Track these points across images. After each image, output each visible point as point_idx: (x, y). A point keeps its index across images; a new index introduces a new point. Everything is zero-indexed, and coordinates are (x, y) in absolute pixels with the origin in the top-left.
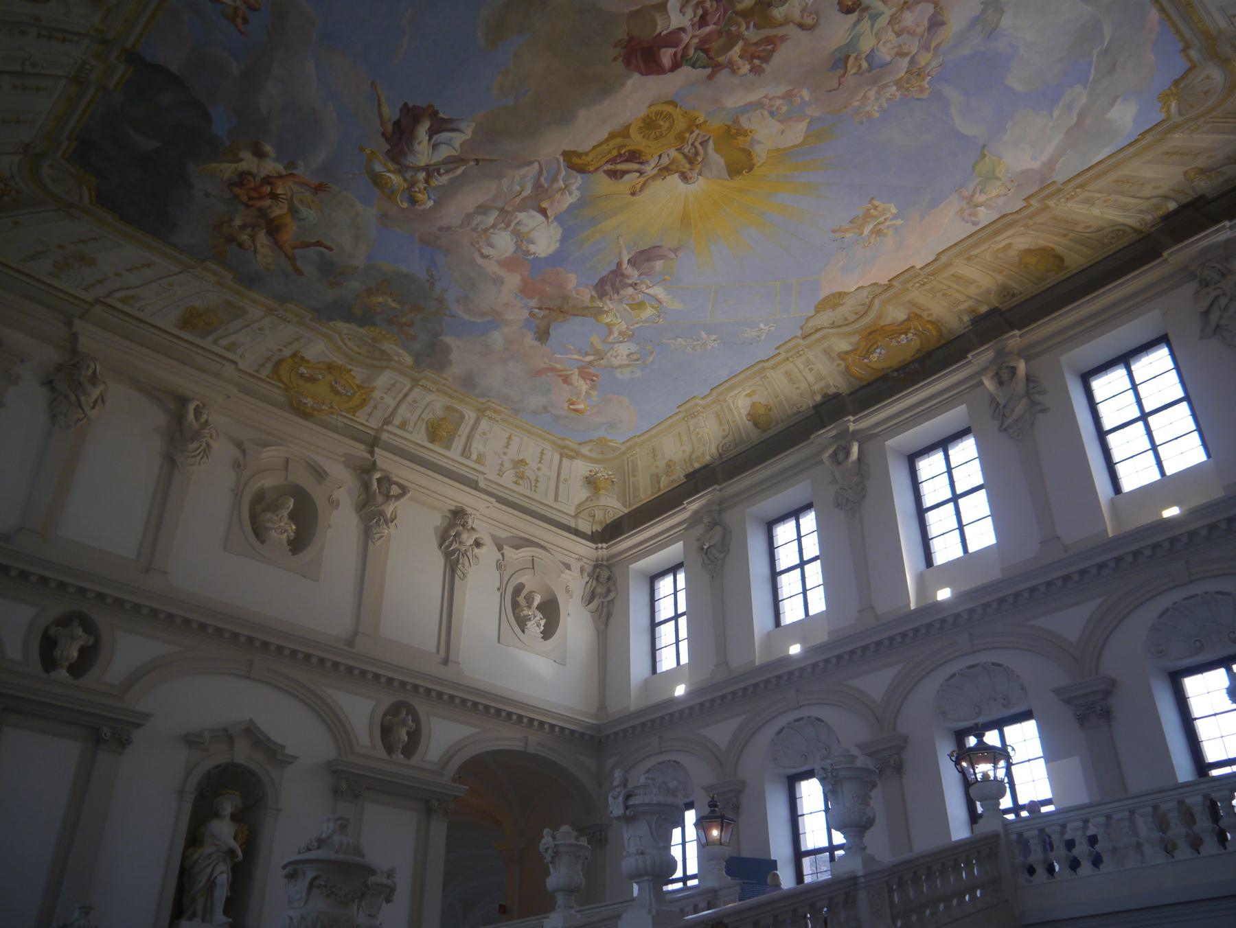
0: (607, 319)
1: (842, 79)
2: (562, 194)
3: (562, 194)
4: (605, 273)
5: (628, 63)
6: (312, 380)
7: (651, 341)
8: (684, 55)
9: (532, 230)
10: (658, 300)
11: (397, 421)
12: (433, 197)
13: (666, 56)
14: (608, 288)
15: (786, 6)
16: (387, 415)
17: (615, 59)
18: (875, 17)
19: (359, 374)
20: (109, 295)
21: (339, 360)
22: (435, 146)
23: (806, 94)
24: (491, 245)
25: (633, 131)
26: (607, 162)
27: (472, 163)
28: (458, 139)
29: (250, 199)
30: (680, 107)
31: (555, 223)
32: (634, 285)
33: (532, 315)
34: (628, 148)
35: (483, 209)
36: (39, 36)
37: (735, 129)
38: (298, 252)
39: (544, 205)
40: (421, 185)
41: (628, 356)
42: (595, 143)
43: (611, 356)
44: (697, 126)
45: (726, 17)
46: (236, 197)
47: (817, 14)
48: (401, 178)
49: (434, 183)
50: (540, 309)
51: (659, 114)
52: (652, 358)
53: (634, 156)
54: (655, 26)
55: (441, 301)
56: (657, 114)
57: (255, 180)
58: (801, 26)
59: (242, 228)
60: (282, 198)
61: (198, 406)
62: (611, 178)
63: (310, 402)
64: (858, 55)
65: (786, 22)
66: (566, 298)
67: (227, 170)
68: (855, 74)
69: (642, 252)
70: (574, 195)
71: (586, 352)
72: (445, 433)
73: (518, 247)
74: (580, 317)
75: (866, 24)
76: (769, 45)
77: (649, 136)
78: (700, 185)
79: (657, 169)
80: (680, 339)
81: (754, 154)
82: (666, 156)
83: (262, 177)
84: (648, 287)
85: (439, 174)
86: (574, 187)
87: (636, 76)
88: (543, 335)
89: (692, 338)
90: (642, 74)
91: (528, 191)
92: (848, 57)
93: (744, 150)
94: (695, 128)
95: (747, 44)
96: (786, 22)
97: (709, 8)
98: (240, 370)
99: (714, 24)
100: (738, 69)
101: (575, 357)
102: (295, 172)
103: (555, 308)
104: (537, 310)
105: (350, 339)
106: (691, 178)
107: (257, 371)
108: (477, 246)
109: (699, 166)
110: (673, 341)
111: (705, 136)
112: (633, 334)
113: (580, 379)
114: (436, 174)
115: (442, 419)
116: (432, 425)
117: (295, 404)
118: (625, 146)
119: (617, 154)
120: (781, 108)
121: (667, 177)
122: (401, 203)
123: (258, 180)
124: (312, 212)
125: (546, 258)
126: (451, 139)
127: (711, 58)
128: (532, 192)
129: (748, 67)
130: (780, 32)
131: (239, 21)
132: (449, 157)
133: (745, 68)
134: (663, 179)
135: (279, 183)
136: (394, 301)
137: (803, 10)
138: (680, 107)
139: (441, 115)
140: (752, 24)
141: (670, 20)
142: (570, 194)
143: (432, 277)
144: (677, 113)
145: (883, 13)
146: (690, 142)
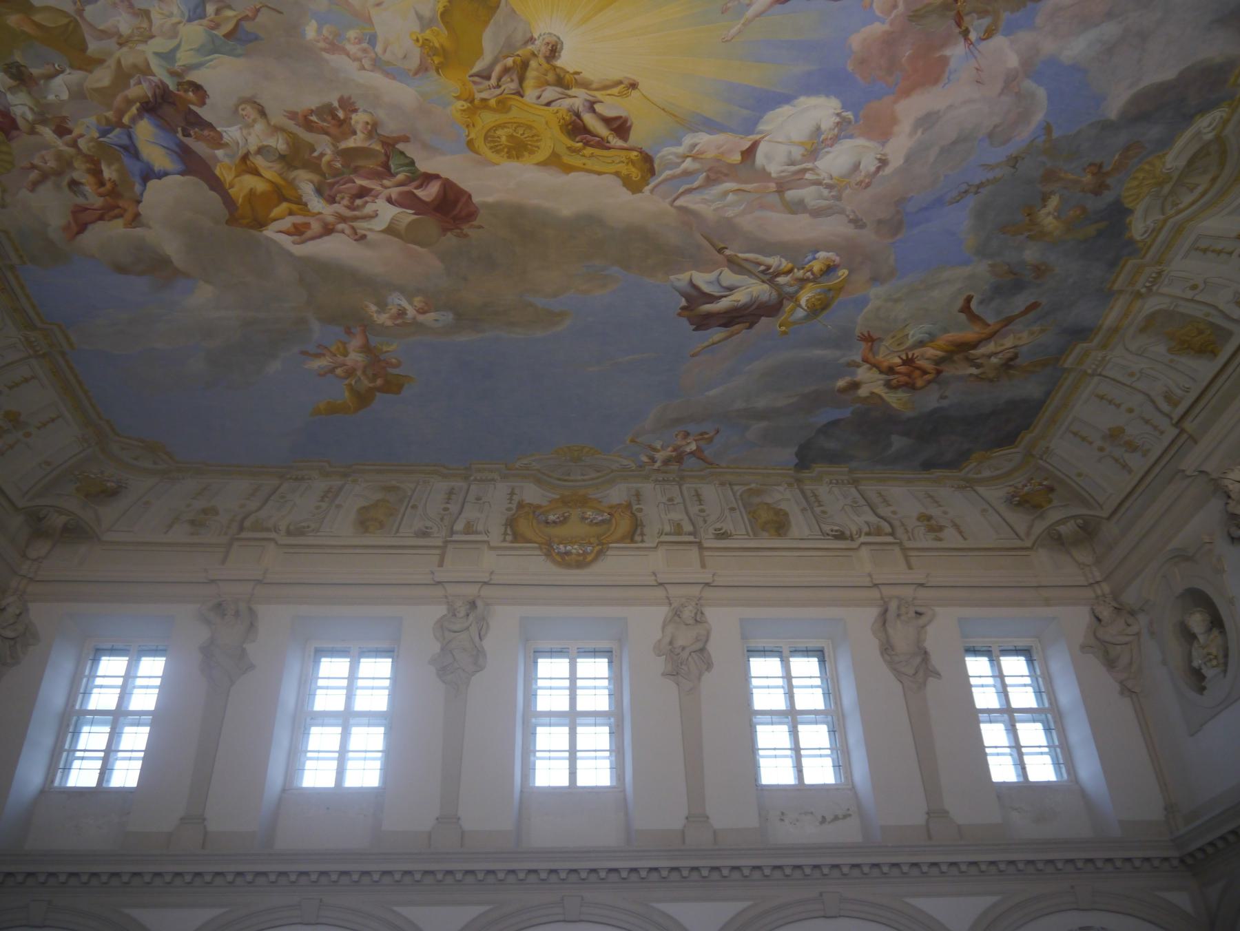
1: (250, 14)
2: (702, 153)
12: (810, 257)
13: (429, 193)
15: (265, 143)
17: (480, 227)
18: (169, 57)
20: (1169, 416)
22: (731, 289)
23: (311, 31)
24: (856, 167)
25: (542, 155)
26: (609, 148)
27: (728, 252)
28: (703, 280)
30: (468, 136)
31: (761, 127)
33: (989, 34)
34: (570, 143)
35: (797, 207)
37: (432, 60)
39: (737, 158)
40: (799, 274)
42: (595, 177)
44: (472, 101)
45: (338, 179)
47: (236, 111)
48: (802, 292)
49: (785, 265)
50: (965, 34)
51: (496, 150)
53: (576, 129)
54: (414, 221)
55: (1014, 161)
56: (498, 152)
58: (263, 113)
59: (978, 366)
62: (630, 127)
64: (213, 28)
65: (278, 129)
67: (895, 400)
68: (229, 7)
70: (696, 140)
73: (836, 139)
75: (183, 58)
76: (312, 121)
77: (533, 136)
78: (545, 26)
79: (570, 92)
82: (542, 97)
86: (681, 150)
87: (476, 199)
90: (470, 196)
91: (729, 185)
92: (228, 36)
93: (446, 23)
94: (476, 102)
95: (336, 140)
96: (278, 129)
97: (347, 198)
99: (354, 182)
100: (367, 123)
103: (953, 13)
104: (973, 36)
106: (548, 44)
108: (867, 180)
109: (518, 53)
111: (474, 83)
114: (771, 271)
118: (569, 148)
120: (356, 38)
121: (571, 71)
122: (840, 277)
123: (891, 377)
124: (911, 333)
126: (710, 283)
129: (354, 116)
130: (291, 125)
131: (706, 436)
132: (735, 273)
133: (359, 119)
135: (886, 364)
136: (1045, 206)
137: (249, 126)
138: (468, 136)
139: (683, 302)
140: (316, 154)
141: (394, 216)
143: (966, 192)
145: (156, 54)
146: (498, 91)
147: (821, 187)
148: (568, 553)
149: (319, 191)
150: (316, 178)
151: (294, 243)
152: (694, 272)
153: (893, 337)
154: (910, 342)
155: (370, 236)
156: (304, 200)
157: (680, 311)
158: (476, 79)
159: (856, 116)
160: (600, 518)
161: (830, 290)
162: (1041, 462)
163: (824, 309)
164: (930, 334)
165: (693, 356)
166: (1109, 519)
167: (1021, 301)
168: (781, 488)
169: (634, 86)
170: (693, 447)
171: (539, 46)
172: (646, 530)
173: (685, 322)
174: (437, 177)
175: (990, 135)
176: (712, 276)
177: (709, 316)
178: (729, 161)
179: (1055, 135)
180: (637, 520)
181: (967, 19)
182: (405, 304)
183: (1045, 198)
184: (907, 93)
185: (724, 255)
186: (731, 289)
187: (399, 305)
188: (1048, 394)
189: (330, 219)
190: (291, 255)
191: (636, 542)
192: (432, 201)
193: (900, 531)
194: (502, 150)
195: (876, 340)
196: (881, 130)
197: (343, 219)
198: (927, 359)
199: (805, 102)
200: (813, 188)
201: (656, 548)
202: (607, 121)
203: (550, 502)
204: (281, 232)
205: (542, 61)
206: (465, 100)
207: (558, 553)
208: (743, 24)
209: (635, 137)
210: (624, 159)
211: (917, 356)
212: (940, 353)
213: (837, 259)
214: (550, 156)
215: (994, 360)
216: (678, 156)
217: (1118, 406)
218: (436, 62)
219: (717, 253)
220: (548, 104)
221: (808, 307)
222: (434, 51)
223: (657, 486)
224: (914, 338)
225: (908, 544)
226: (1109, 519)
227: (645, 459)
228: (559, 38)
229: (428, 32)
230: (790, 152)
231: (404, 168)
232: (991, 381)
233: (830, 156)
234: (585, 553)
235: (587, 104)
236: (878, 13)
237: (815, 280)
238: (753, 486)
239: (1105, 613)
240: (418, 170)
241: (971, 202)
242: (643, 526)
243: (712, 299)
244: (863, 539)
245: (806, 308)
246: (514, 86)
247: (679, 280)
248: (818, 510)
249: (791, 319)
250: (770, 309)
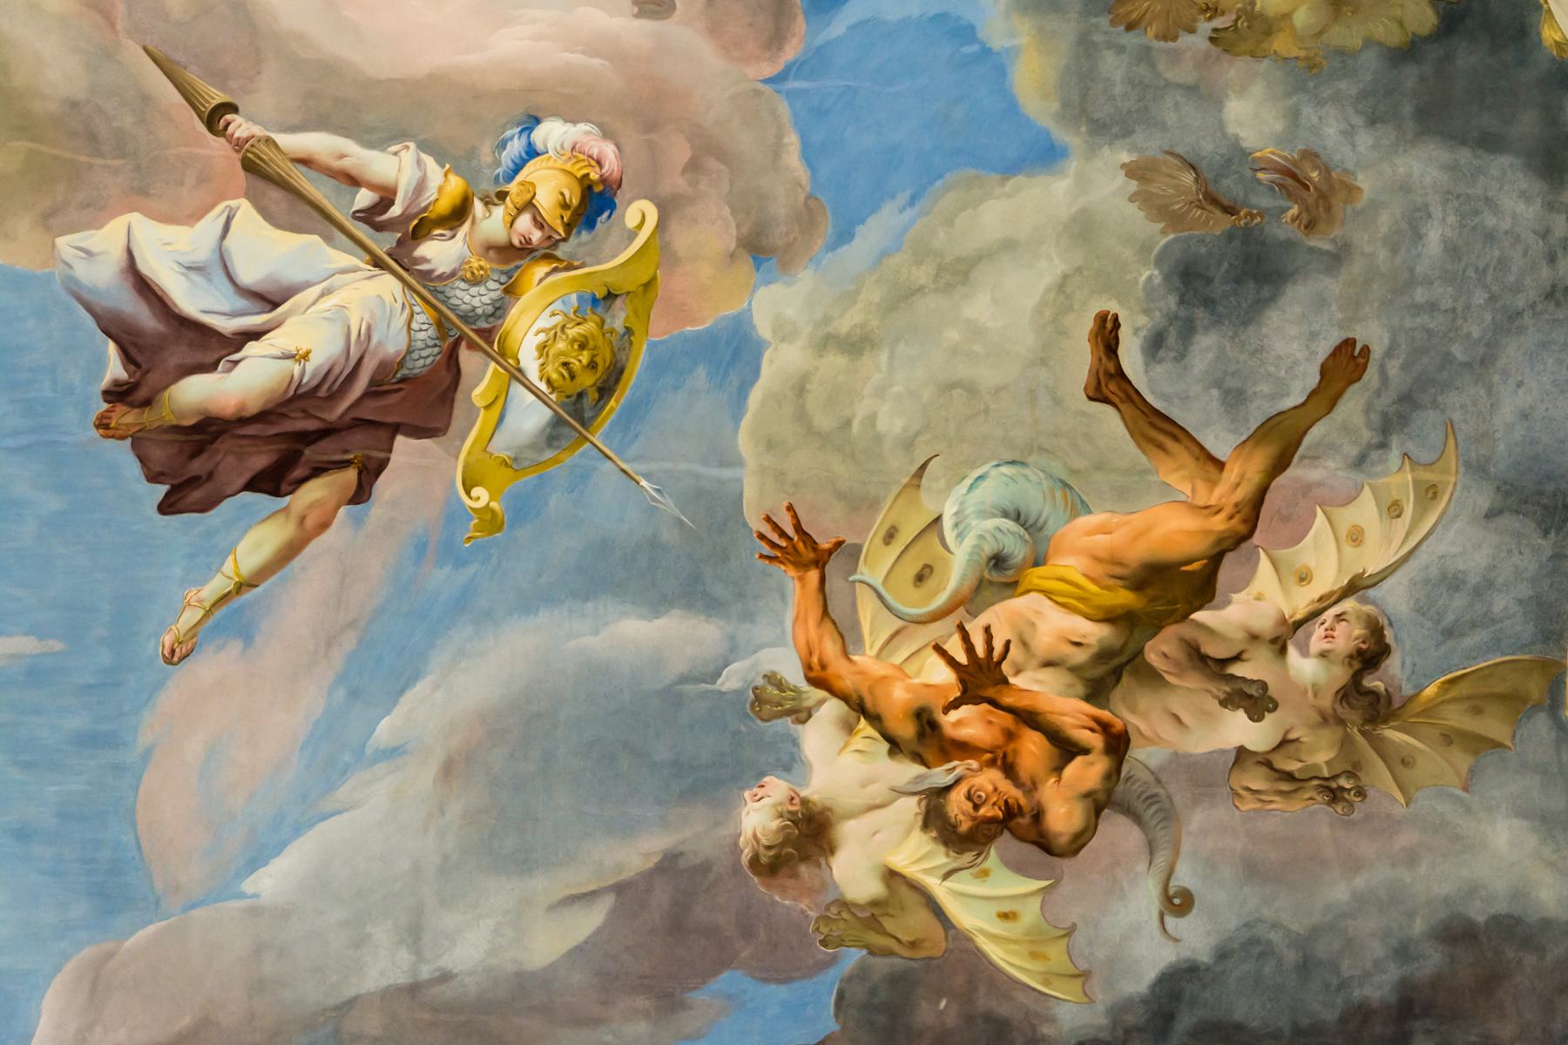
12: (516, 147)
22: (269, 299)
27: (240, 126)
29: (1066, 749)
38: (1220, 442)
40: (491, 223)
46: (1099, 804)
48: (514, 311)
49: (443, 187)
57: (958, 781)
59: (1256, 702)
60: (970, 649)
83: (918, 769)
85: (386, 202)
102: (794, 675)
114: (396, 211)
122: (632, 235)
123: (940, 776)
132: (278, 225)
135: (898, 699)
139: (115, 369)
152: (135, 218)
153: (890, 536)
154: (957, 569)
157: (105, 406)
161: (610, 296)
163: (606, 390)
164: (1017, 517)
165: (172, 658)
173: (122, 454)
176: (197, 239)
185: (229, 139)
195: (830, 552)
198: (1048, 664)
211: (1008, 644)
212: (1096, 633)
215: (1304, 667)
219: (201, 128)
221: (549, 382)
224: (969, 541)
237: (547, 252)
245: (543, 386)
247: (89, 253)
249: (502, 445)
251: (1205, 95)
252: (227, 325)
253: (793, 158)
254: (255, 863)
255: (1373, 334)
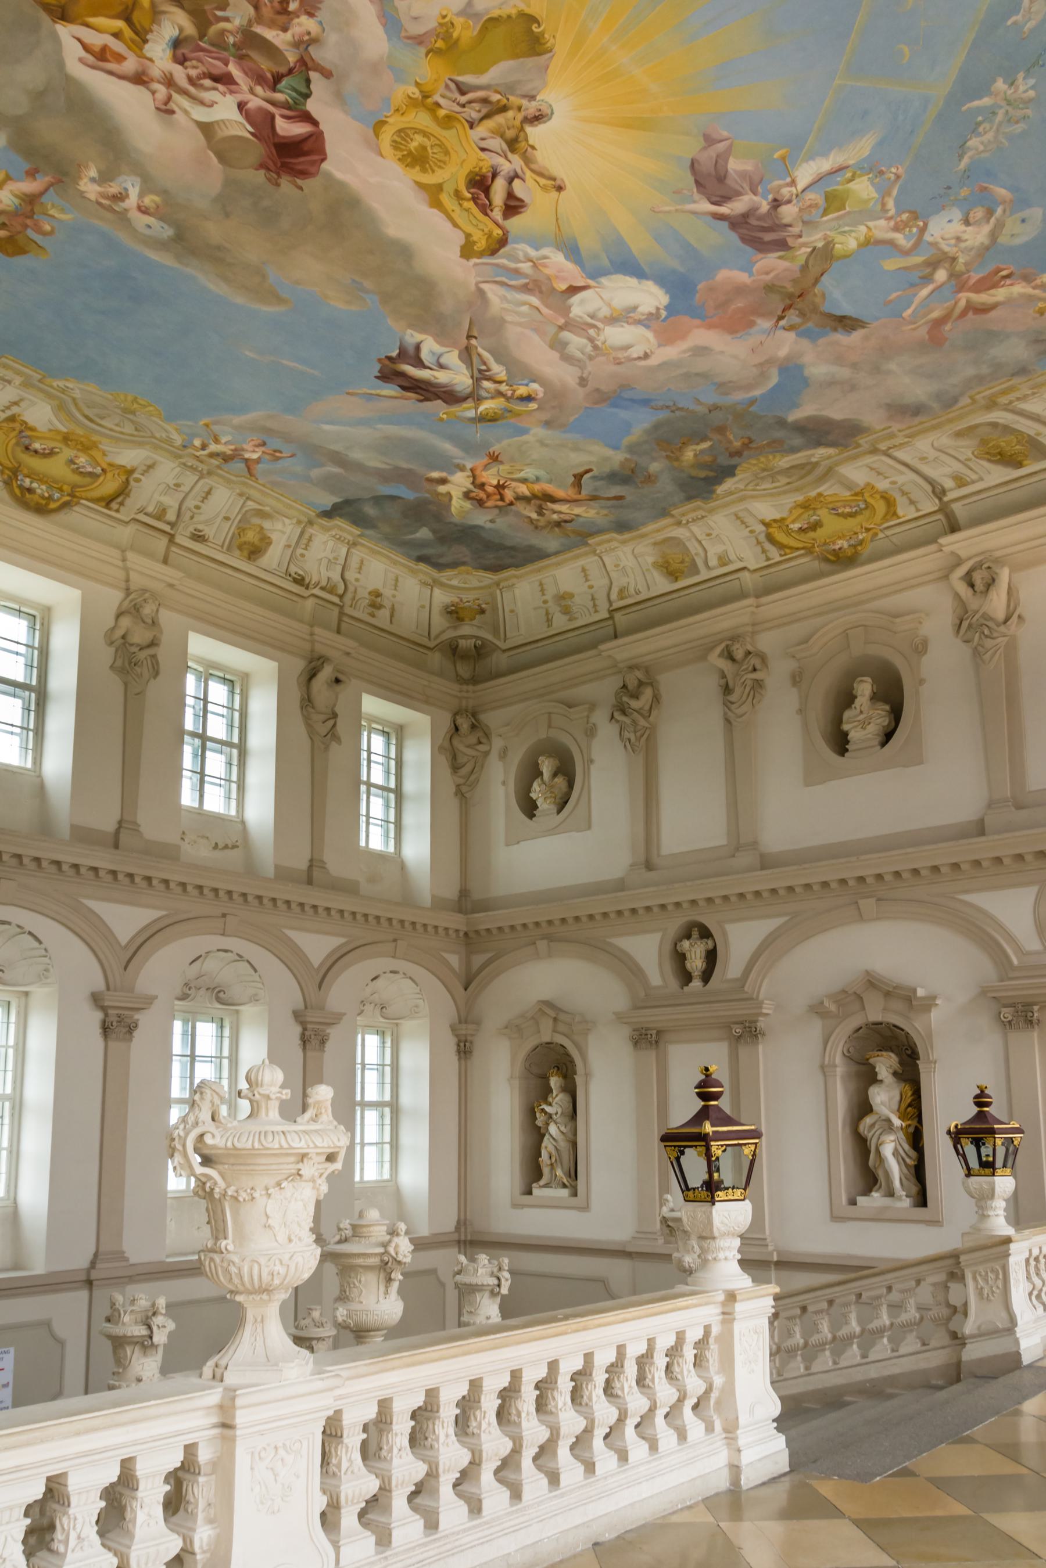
0: (848, 243)
3: (545, 266)
4: (733, 237)
5: (304, 174)
6: (815, 526)
7: (949, 188)
8: (286, 106)
9: (609, 305)
10: (841, 169)
11: (948, 484)
12: (525, 382)
13: (287, 128)
14: (768, 237)
16: (929, 488)
17: (301, 188)
19: (827, 489)
20: (611, 603)
21: (800, 498)
22: (441, 366)
26: (486, 214)
27: (473, 342)
28: (430, 347)
31: (604, 280)
32: (776, 203)
33: (790, 328)
35: (558, 345)
36: (306, 549)
38: (584, 492)
40: (503, 388)
41: (967, 222)
43: (956, 246)
44: (426, 96)
46: (496, 507)
49: (502, 375)
51: (396, 146)
52: (1002, 192)
55: (714, 408)
59: (540, 513)
61: (727, 646)
63: (842, 543)
66: (770, 288)
67: (458, 505)
69: (697, 182)
70: (551, 255)
71: (921, 278)
72: (1018, 447)
73: (639, 322)
74: (823, 278)
79: (510, 155)
80: (969, 144)
81: (495, 13)
84: (793, 183)
86: (532, 253)
87: (325, 166)
88: (846, 323)
89: (979, 124)
90: (323, 160)
91: (535, 301)
94: (429, 100)
95: (259, 19)
98: (755, 570)
99: (226, 64)
100: (309, 33)
101: (925, 292)
104: (782, 323)
105: (757, 485)
107: (768, 559)
109: (511, 98)
110: (970, 154)
112: (910, 212)
113: (992, 291)
115: (983, 442)
116: (988, 453)
117: (832, 558)
119: (472, 203)
121: (531, 142)
125: (671, 298)
127: (290, 71)
128: (534, 295)
129: (304, 19)
131: (278, 454)
133: (304, 24)
134: (533, 148)
135: (484, 480)
136: (698, 444)
139: (394, 354)
140: (219, 13)
142: (546, 257)
143: (668, 407)
144: (396, 122)
146: (458, 109)
147: (590, 344)
148: (30, 490)
149: (176, 43)
150: (190, 29)
151: (81, 60)
155: (179, 116)
156: (148, 37)
158: (452, 86)
159: (666, 318)
160: (90, 469)
162: (498, 592)
163: (490, 421)
165: (348, 393)
166: (504, 651)
167: (616, 490)
168: (287, 521)
169: (560, 189)
170: (255, 456)
171: (531, 108)
172: (128, 502)
173: (378, 366)
174: (315, 123)
175: (721, 385)
176: (438, 348)
177: (403, 375)
178: (555, 285)
179: (752, 409)
180: (126, 487)
181: (792, 311)
182: (134, 193)
183: (704, 439)
184: (710, 327)
186: (441, 366)
187: (126, 189)
188: (557, 553)
189: (155, 72)
190: (61, 65)
191: (110, 509)
192: (284, 137)
193: (349, 596)
194: (401, 150)
196: (666, 338)
197: (169, 82)
199: (650, 286)
200: (585, 341)
201: (127, 523)
202: (510, 195)
203: (50, 430)
204: (79, 40)
205: (520, 117)
206: (421, 92)
207: (20, 487)
208: (677, 210)
209: (515, 224)
210: (486, 230)
212: (527, 493)
213: (541, 395)
214: (434, 185)
216: (526, 255)
217: (587, 580)
218: (437, 45)
220: (483, 150)
222: (447, 37)
223: (179, 469)
225: (348, 610)
226: (504, 651)
227: (197, 443)
228: (552, 113)
229: (462, 20)
230: (600, 309)
231: (294, 94)
232: (536, 527)
233: (620, 329)
234: (50, 498)
235: (512, 174)
236: (754, 270)
237: (508, 399)
238: (267, 509)
239: (464, 724)
240: (305, 105)
241: (663, 415)
242: (128, 495)
243: (420, 363)
244: (317, 591)
246: (475, 115)
248: (299, 551)
250: (450, 396)
251: (654, 459)
252: (426, 363)
253: (572, 419)
254: (327, 423)
255: (629, 498)
